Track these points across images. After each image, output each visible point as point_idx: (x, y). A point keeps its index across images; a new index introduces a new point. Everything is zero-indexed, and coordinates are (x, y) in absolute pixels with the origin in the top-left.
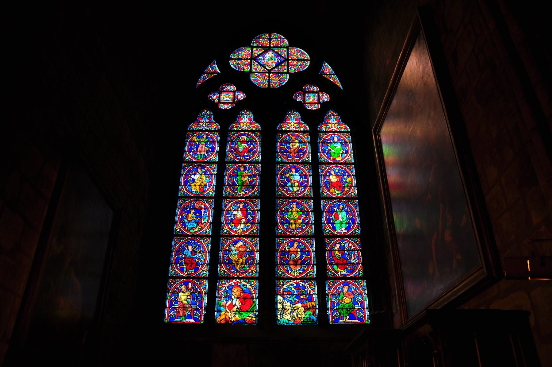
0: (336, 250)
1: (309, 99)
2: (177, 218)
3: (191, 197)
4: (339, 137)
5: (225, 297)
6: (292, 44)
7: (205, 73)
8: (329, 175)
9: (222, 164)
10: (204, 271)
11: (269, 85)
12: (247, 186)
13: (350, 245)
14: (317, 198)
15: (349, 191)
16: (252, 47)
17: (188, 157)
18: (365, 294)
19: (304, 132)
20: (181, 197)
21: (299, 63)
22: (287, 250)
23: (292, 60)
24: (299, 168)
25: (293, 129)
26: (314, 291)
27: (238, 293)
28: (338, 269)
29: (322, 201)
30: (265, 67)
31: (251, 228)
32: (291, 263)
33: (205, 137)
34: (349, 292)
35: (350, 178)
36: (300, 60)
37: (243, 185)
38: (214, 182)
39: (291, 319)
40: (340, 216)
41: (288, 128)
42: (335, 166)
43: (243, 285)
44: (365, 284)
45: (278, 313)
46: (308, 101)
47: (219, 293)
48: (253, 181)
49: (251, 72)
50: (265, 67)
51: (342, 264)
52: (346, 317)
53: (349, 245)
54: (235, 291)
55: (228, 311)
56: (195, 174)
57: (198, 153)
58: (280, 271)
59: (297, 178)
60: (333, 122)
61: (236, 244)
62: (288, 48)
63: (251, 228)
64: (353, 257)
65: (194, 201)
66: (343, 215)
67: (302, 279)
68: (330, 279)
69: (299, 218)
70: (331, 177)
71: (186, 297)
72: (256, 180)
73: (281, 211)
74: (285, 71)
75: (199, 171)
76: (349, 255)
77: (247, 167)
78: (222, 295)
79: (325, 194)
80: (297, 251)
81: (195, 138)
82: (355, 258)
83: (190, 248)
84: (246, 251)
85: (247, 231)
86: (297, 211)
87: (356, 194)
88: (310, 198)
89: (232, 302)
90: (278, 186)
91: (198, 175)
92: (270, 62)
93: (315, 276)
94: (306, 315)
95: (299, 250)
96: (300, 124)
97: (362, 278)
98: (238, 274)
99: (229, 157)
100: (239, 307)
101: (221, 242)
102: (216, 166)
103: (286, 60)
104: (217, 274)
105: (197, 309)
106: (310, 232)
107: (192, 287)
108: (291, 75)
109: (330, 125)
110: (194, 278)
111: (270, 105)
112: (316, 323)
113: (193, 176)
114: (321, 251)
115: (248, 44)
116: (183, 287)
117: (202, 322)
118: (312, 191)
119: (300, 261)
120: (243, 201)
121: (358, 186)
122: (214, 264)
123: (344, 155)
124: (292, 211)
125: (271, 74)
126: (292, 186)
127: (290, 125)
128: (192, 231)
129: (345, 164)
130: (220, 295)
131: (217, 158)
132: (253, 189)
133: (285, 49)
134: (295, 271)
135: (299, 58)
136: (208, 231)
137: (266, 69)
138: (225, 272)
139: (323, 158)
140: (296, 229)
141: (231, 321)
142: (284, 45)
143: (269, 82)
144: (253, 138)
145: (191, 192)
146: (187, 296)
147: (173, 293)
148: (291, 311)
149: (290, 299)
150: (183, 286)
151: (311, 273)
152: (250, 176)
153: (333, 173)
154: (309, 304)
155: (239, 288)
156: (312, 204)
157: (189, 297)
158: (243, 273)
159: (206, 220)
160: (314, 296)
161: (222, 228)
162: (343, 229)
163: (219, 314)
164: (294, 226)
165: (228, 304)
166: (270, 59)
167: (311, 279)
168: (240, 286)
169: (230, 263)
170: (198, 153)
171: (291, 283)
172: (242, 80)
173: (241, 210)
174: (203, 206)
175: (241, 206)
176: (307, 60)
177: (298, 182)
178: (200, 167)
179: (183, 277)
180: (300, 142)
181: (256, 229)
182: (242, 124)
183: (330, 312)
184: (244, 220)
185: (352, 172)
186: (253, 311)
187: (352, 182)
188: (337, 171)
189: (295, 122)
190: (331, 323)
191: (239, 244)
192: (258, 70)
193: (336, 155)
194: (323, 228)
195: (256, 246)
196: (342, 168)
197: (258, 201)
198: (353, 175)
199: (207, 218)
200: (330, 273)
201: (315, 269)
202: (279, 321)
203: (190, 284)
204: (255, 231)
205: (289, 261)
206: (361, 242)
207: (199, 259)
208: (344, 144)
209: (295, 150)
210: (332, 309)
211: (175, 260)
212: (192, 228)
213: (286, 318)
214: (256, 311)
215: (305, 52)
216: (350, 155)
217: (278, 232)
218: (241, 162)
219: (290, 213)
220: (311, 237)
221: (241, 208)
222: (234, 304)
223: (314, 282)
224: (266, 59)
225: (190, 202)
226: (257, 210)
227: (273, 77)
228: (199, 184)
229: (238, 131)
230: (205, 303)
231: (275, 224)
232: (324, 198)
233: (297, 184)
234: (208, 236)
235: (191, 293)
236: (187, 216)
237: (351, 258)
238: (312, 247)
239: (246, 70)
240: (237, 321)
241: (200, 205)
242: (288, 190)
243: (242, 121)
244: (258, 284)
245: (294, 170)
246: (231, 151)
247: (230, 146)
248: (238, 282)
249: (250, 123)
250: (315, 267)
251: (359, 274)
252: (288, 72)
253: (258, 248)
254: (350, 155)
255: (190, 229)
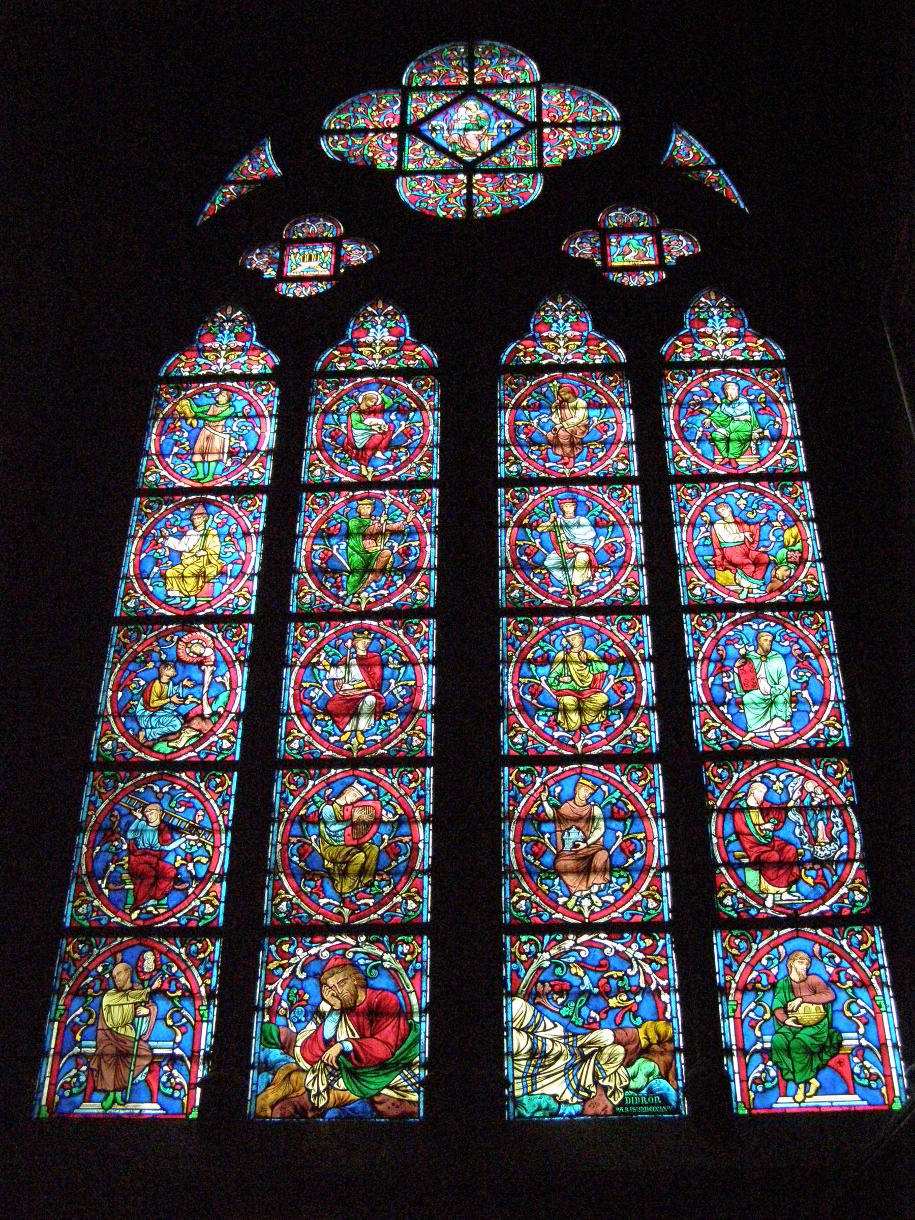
0: (749, 808)
1: (623, 254)
2: (106, 698)
3: (163, 620)
4: (744, 384)
5: (291, 1008)
6: (553, 75)
7: (231, 183)
8: (712, 523)
9: (285, 495)
10: (210, 903)
11: (470, 212)
12: (383, 571)
13: (810, 786)
14: (666, 607)
15: (794, 578)
16: (406, 92)
17: (153, 475)
18: (882, 984)
19: (607, 369)
20: (123, 621)
21: (582, 134)
22: (549, 811)
23: (554, 125)
24: (591, 497)
25: (563, 355)
26: (662, 972)
27: (345, 991)
28: (765, 885)
29: (687, 618)
30: (452, 155)
31: (403, 728)
32: (566, 863)
33: (223, 398)
34: (813, 979)
35: (795, 530)
36: (586, 125)
37: (367, 569)
38: (255, 563)
39: (568, 1096)
40: (761, 674)
41: (545, 357)
42: (733, 489)
43: (369, 955)
44: (880, 945)
45: (516, 1069)
46: (617, 262)
47: (266, 994)
48: (406, 552)
49: (400, 171)
50: (452, 155)
51: (780, 864)
52: (807, 1083)
53: (802, 785)
54: (331, 981)
55: (304, 1065)
56: (182, 534)
57: (197, 458)
58: (518, 900)
59: (584, 533)
60: (718, 331)
61: (340, 794)
62: (537, 86)
63: (403, 728)
64: (822, 836)
65: (173, 632)
66: (774, 670)
67: (615, 929)
68: (728, 925)
69: (595, 687)
70: (719, 527)
71: (129, 1009)
72: (422, 547)
73: (522, 660)
74: (529, 164)
75: (198, 520)
76: (806, 825)
77: (387, 501)
78: (278, 1001)
79: (697, 591)
80: (591, 819)
81: (185, 406)
82: (832, 839)
83: (154, 816)
84: (378, 821)
85: (384, 742)
86: (589, 662)
87: (824, 588)
88: (636, 611)
89: (320, 1027)
90: (507, 568)
91: (192, 539)
92: (471, 136)
93: (667, 916)
94: (634, 1077)
95: (597, 812)
96: (588, 341)
97: (865, 920)
98: (346, 912)
99: (315, 469)
100: (349, 1046)
101: (278, 787)
102: (262, 501)
103: (528, 126)
104: (261, 915)
105: (173, 1060)
106: (640, 738)
107: (158, 969)
108: (552, 176)
109: (709, 342)
110: (169, 933)
111: (470, 288)
112: (677, 1110)
113: (172, 543)
114: (688, 814)
115: (388, 80)
116: (121, 972)
117: (194, 1115)
118: (644, 580)
119: (601, 859)
120: (369, 629)
121: (828, 557)
122: (247, 874)
123: (766, 448)
124: (564, 661)
125: (478, 176)
126: (564, 568)
127: (551, 345)
128: (162, 747)
129: (775, 477)
130: (269, 1002)
131: (269, 474)
132: (408, 582)
133: (527, 92)
134: (587, 897)
135: (581, 117)
136: (226, 744)
137: (460, 160)
138: (292, 906)
139: (682, 458)
140: (584, 729)
141: (315, 1108)
142: (523, 78)
143: (469, 202)
144: (410, 396)
145: (162, 603)
146: (136, 1005)
147: (79, 992)
148: (571, 1064)
149: (565, 1012)
150: (120, 967)
151: (652, 904)
152: (394, 533)
153: (726, 512)
154: (646, 1032)
155: (350, 970)
156: (647, 631)
157: (144, 1011)
158: (371, 910)
159: (218, 706)
160: (665, 997)
161: (282, 731)
162: (778, 723)
163: (265, 1077)
164: (574, 717)
165: (300, 1040)
166: (471, 132)
167: (649, 928)
168: (353, 964)
169: (312, 872)
170: (197, 458)
171: (568, 944)
172: (363, 199)
173: (363, 663)
174: (209, 652)
175: (361, 646)
176: (611, 124)
177: (588, 550)
178: (201, 509)
179: (121, 931)
180: (591, 405)
181: (424, 736)
182: (366, 351)
183: (734, 1065)
184: (370, 700)
185: (802, 507)
186: (409, 1066)
187: (805, 547)
188: (742, 503)
189: (570, 334)
190: (743, 1111)
191: (350, 796)
192: (425, 165)
193: (734, 447)
194: (696, 723)
195: (421, 799)
196: (763, 493)
197: (429, 628)
198: (808, 520)
199: (223, 697)
200: (728, 901)
201: (667, 887)
202: (517, 1102)
203: (149, 957)
204: (416, 741)
205: (557, 857)
206: (857, 775)
207: (189, 857)
208: (765, 406)
209: (572, 436)
210: (743, 1052)
211: (91, 859)
212: (165, 737)
213: (550, 1092)
214: (424, 1066)
215: (601, 98)
216: (792, 446)
217: (510, 742)
218: (362, 484)
219: (559, 668)
220: (645, 758)
221: (361, 653)
222: (328, 1033)
223: (665, 942)
224: (460, 125)
225: (157, 638)
226: (427, 662)
227: (485, 186)
228: (194, 569)
229: (351, 374)
230: (207, 1030)
231: (498, 711)
232: (694, 608)
233: (583, 558)
234: (226, 766)
235: (152, 994)
236: (145, 693)
237: (813, 840)
238: (651, 798)
239: (384, 166)
240: (341, 1105)
241: (198, 649)
242: (547, 580)
243: (370, 339)
244: (427, 953)
245: (569, 508)
246: (321, 447)
247: (320, 428)
248: (345, 947)
249: (398, 344)
250: (666, 877)
251: (854, 903)
252: (540, 168)
253: (430, 809)
254: (792, 446)
255: (156, 741)
